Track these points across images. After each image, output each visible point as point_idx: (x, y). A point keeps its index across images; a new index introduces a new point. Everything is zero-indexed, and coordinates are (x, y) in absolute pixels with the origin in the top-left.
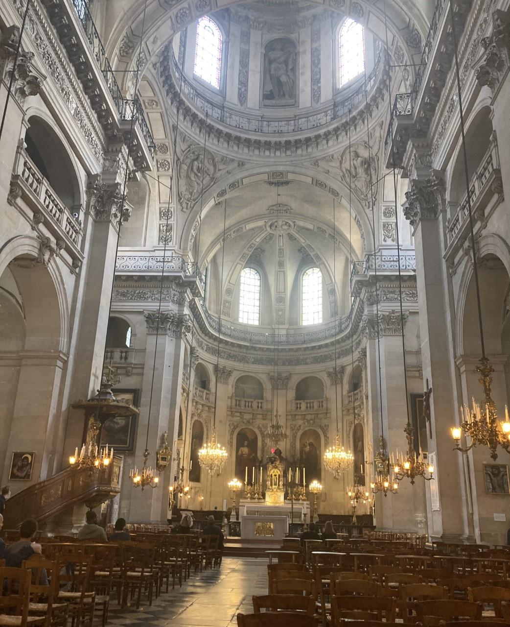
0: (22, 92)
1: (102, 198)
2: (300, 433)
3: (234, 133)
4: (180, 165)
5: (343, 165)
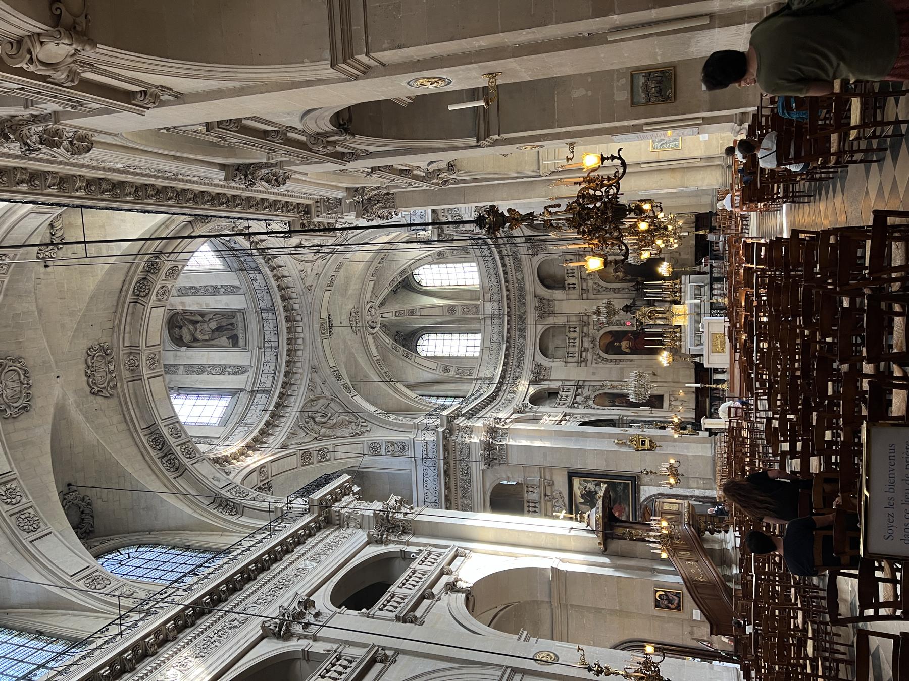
0: (317, 615)
1: (389, 529)
2: (602, 283)
3: (281, 379)
5: (311, 259)
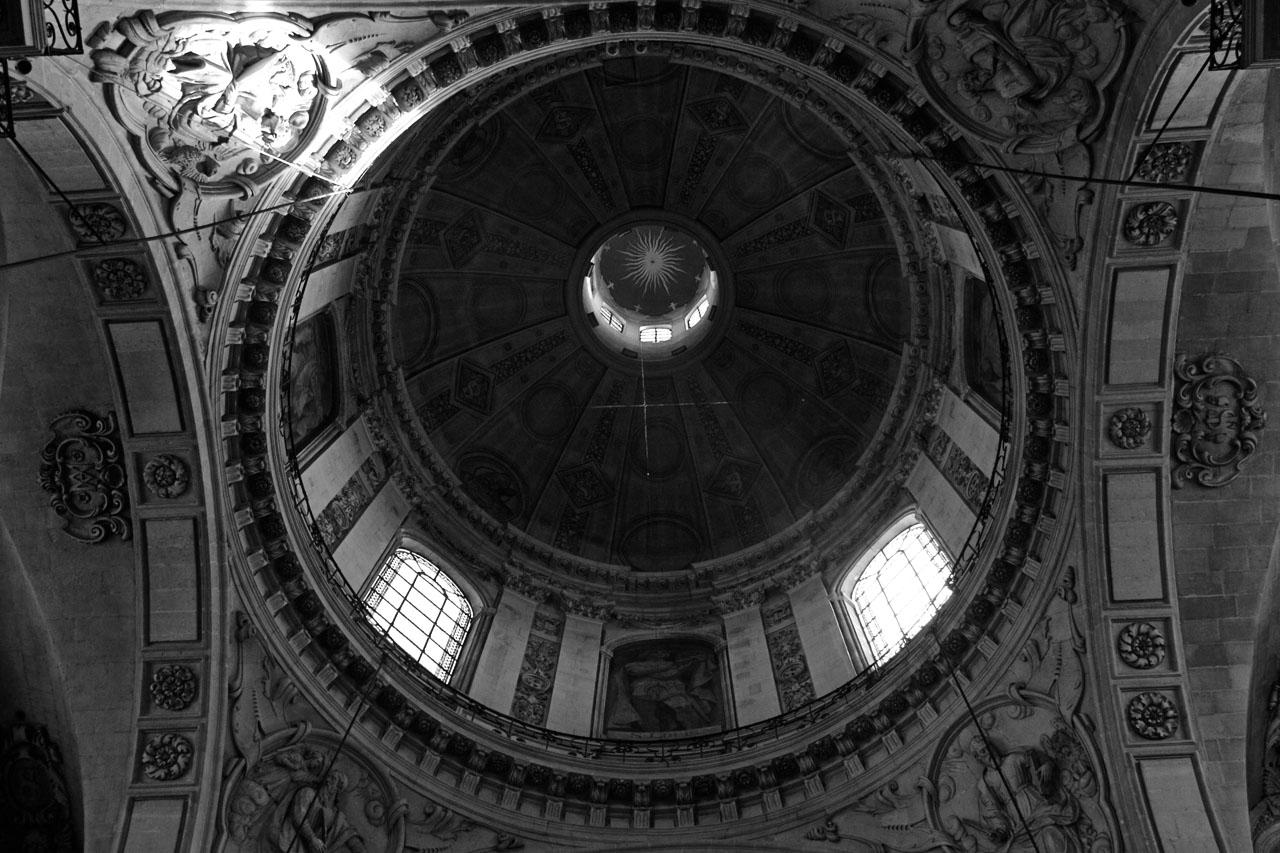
4: (237, 793)
5: (945, 812)
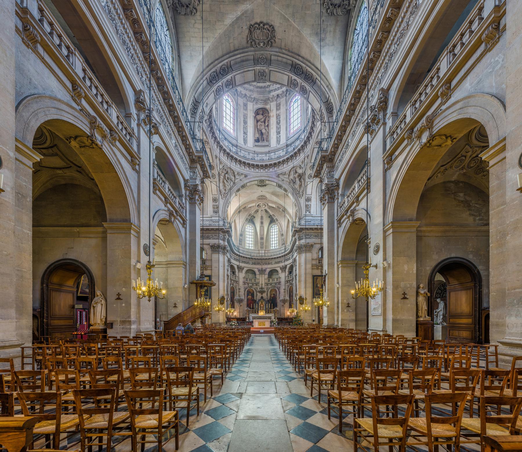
3: (243, 160)
